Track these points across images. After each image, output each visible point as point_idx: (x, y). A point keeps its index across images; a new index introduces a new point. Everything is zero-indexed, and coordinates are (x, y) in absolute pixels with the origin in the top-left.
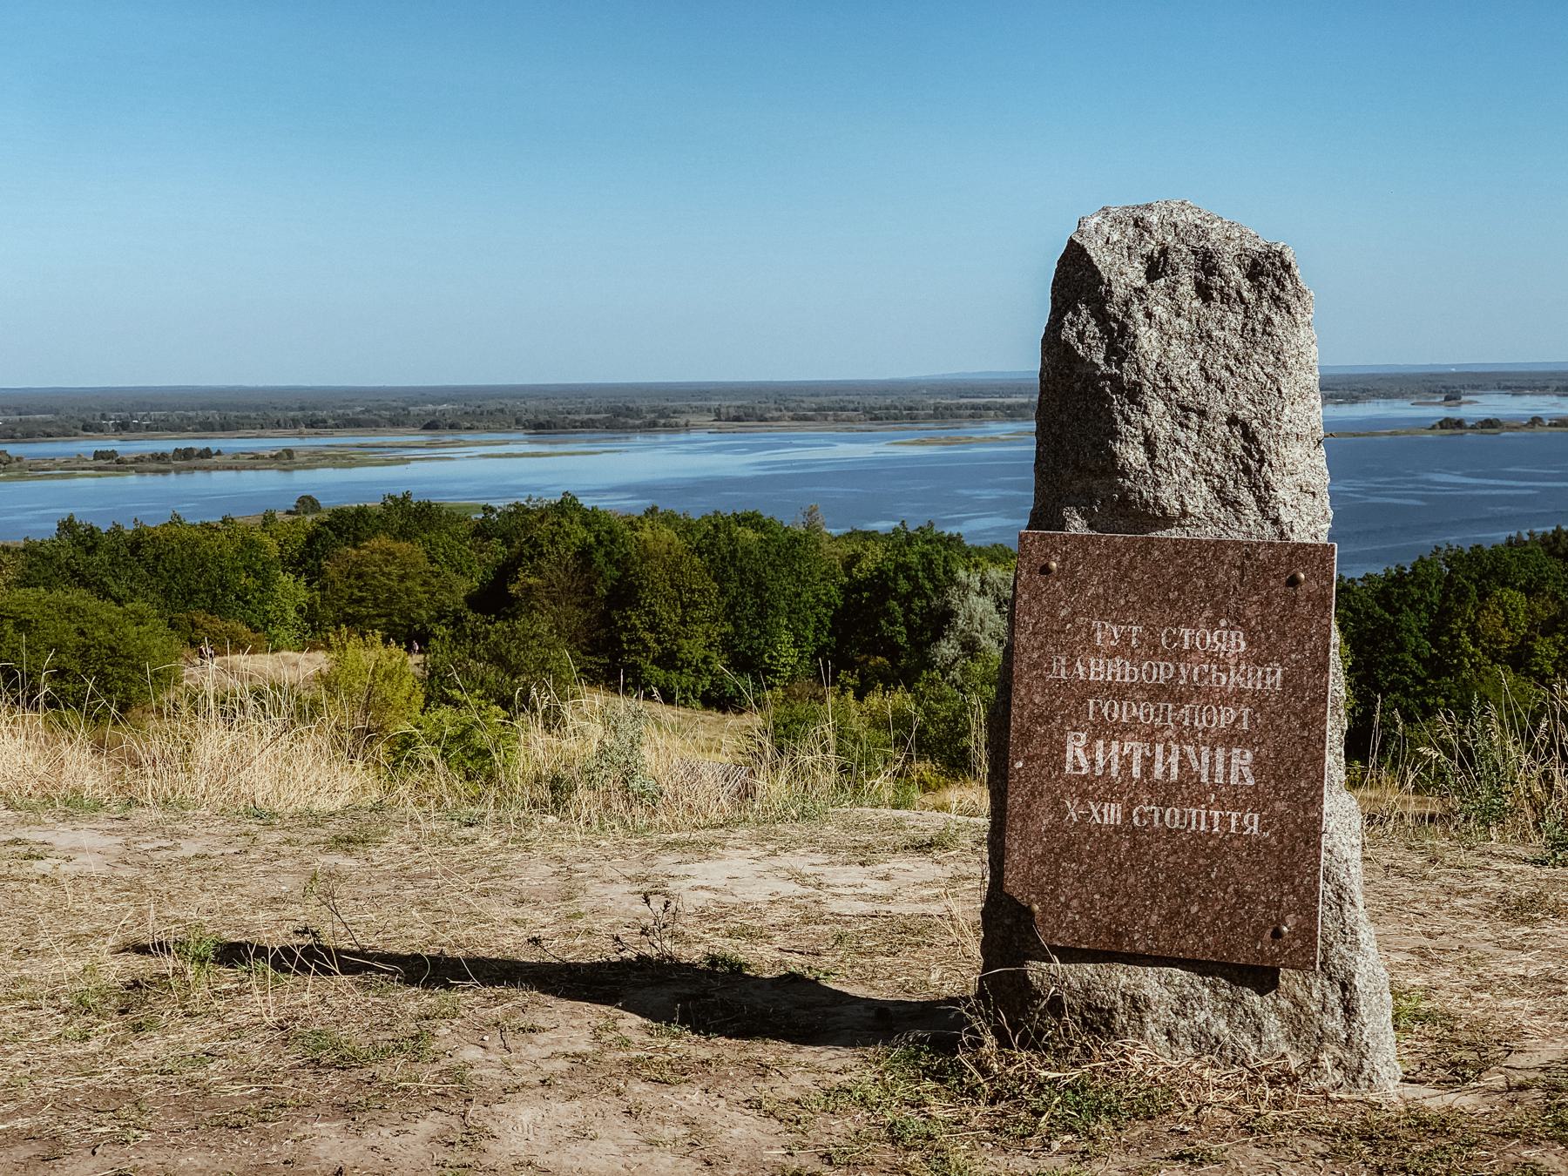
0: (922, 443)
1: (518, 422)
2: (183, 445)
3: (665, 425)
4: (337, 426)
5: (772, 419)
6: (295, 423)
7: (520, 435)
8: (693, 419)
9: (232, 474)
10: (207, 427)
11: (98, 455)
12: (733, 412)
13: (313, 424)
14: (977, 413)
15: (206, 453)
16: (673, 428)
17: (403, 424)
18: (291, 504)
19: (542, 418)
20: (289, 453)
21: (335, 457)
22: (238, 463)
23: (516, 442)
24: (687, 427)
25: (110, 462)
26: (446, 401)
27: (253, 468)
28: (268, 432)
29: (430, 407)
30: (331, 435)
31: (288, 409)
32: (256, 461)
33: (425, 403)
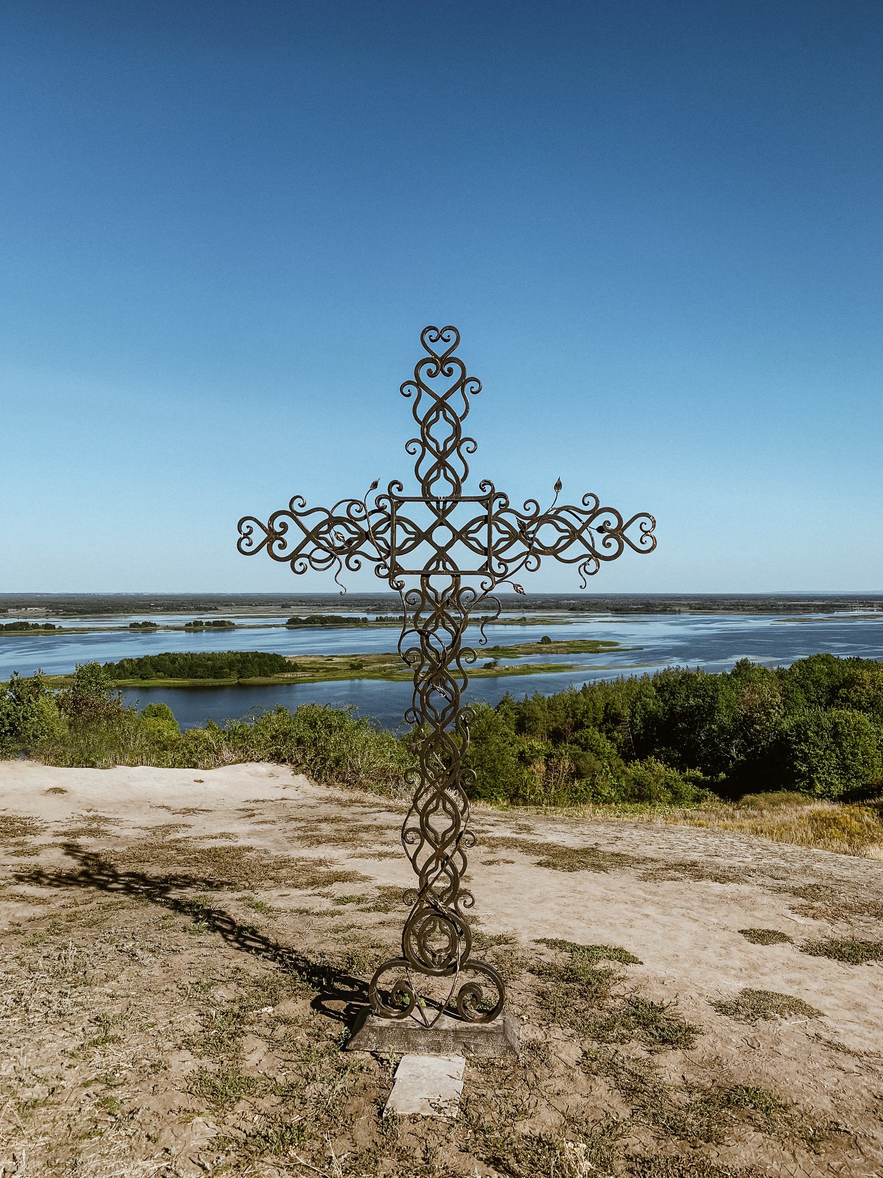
0: (789, 621)
2: (484, 615)
4: (535, 608)
5: (715, 609)
6: (519, 607)
7: (610, 614)
8: (682, 609)
9: (503, 626)
12: (697, 606)
13: (526, 607)
14: (806, 609)
16: (674, 612)
17: (561, 608)
18: (539, 640)
19: (618, 607)
20: (524, 619)
21: (542, 621)
22: (505, 622)
23: (607, 616)
24: (679, 612)
26: (572, 599)
27: (512, 624)
28: (510, 611)
30: (534, 612)
31: (512, 601)
32: (512, 622)
33: (565, 600)
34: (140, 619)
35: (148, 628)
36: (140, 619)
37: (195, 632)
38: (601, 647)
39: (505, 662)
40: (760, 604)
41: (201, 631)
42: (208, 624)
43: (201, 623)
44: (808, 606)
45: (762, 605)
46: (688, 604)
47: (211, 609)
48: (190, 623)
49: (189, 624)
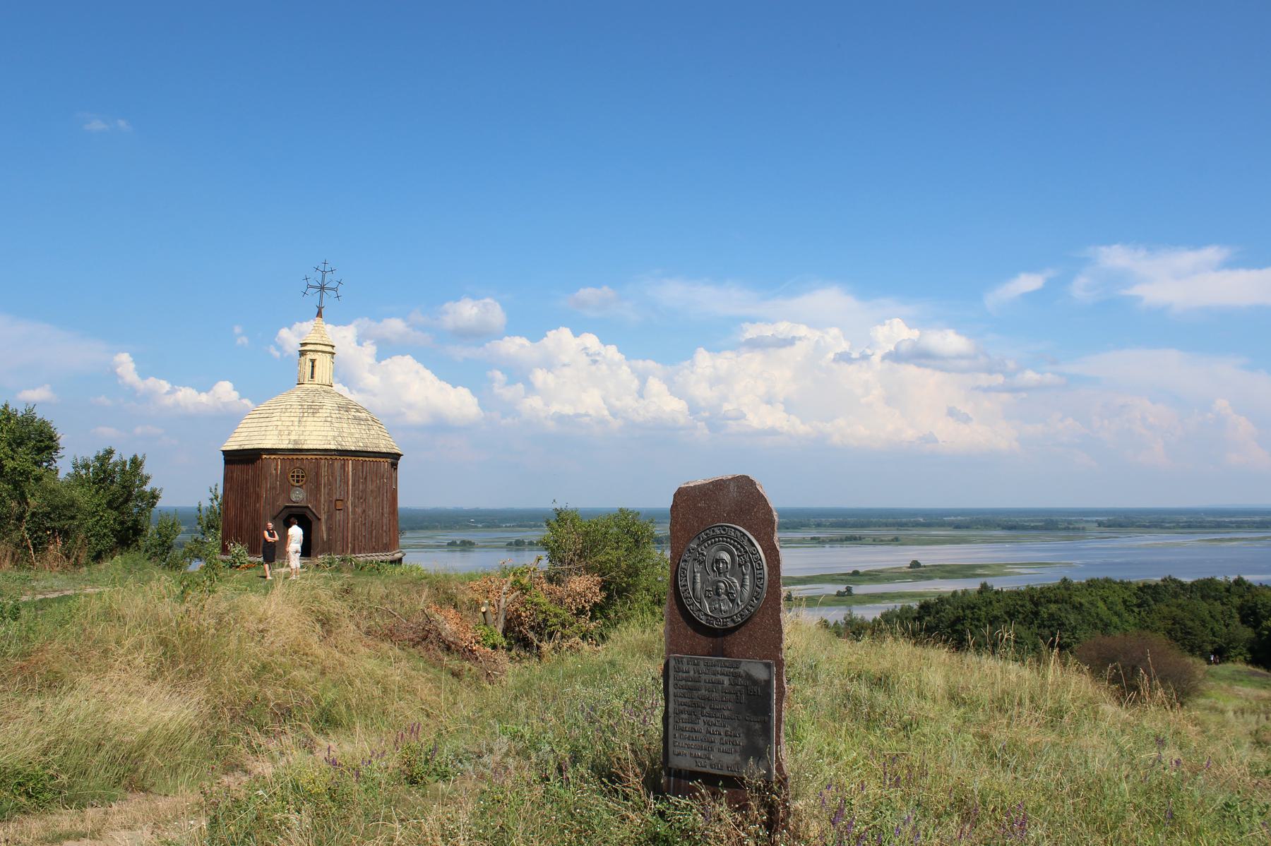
1: (999, 526)
3: (1073, 529)
10: (855, 526)
11: (813, 539)
15: (860, 539)
25: (817, 541)
29: (952, 518)
33: (950, 516)
34: (458, 536)
35: (466, 546)
36: (458, 536)
37: (518, 550)
38: (979, 571)
39: (859, 590)
40: (1185, 519)
41: (523, 550)
42: (531, 543)
43: (523, 542)
44: (1242, 522)
45: (1186, 522)
46: (1097, 521)
47: (535, 526)
48: (511, 542)
49: (510, 544)
